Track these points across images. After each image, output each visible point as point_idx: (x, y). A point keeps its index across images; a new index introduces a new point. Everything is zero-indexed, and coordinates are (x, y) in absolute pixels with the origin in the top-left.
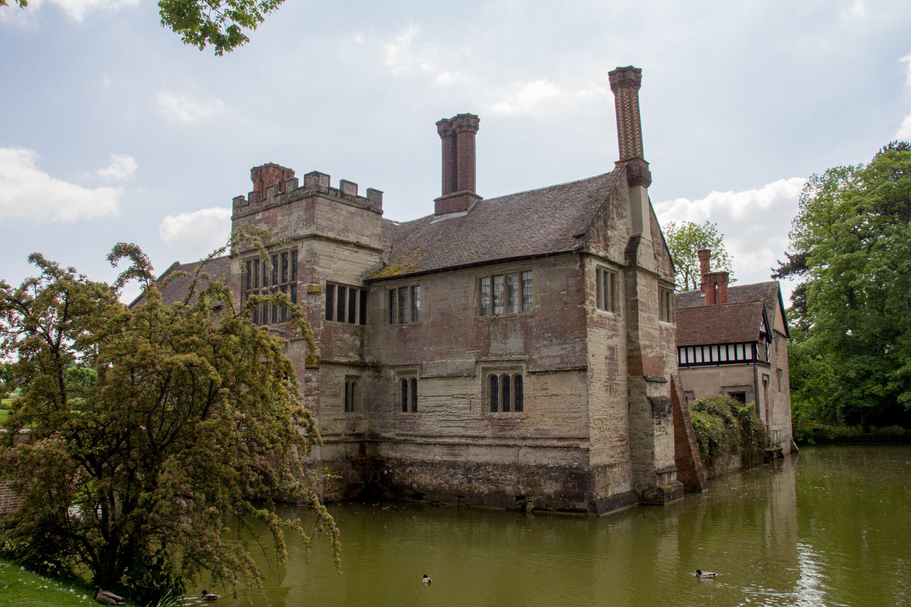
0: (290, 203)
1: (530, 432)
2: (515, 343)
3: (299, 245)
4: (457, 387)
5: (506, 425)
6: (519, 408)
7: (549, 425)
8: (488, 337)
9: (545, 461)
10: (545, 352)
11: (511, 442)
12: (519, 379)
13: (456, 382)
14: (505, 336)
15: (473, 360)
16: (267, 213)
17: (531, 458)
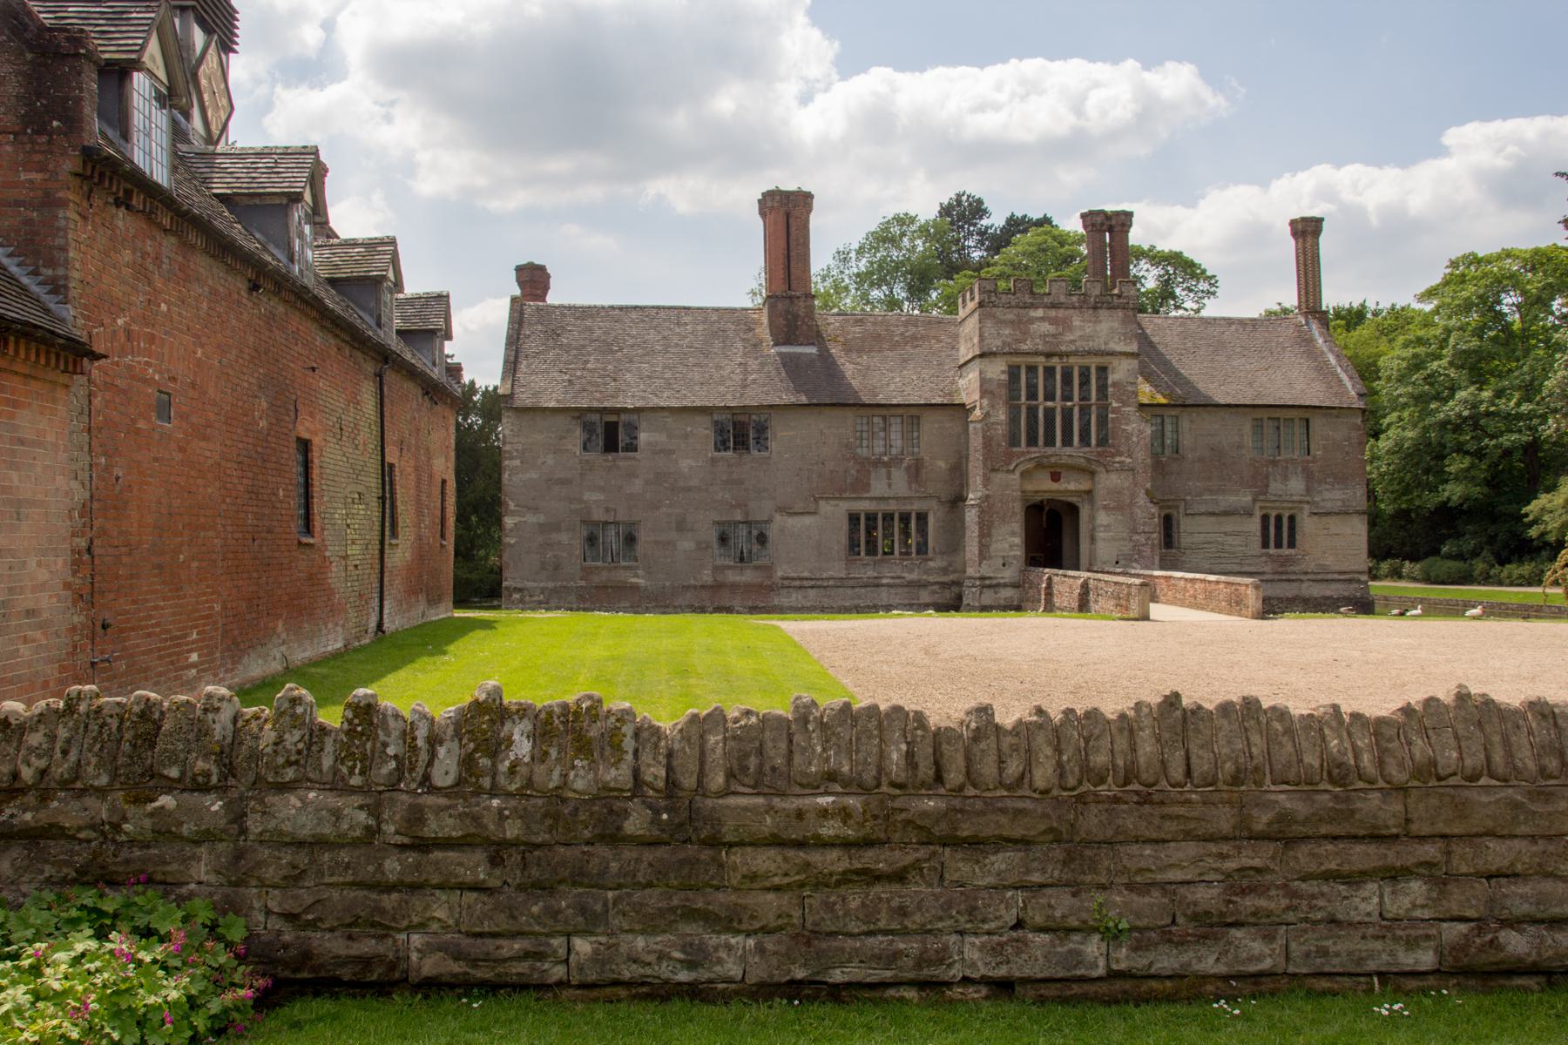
0: (1095, 308)
1: (1312, 567)
2: (1296, 485)
3: (1115, 361)
4: (1230, 525)
5: (1288, 560)
6: (1292, 544)
7: (1329, 561)
8: (1267, 477)
9: (1328, 593)
10: (1327, 495)
11: (1293, 577)
12: (1292, 519)
13: (1233, 518)
14: (1286, 478)
15: (1249, 498)
16: (1053, 313)
17: (1316, 591)
